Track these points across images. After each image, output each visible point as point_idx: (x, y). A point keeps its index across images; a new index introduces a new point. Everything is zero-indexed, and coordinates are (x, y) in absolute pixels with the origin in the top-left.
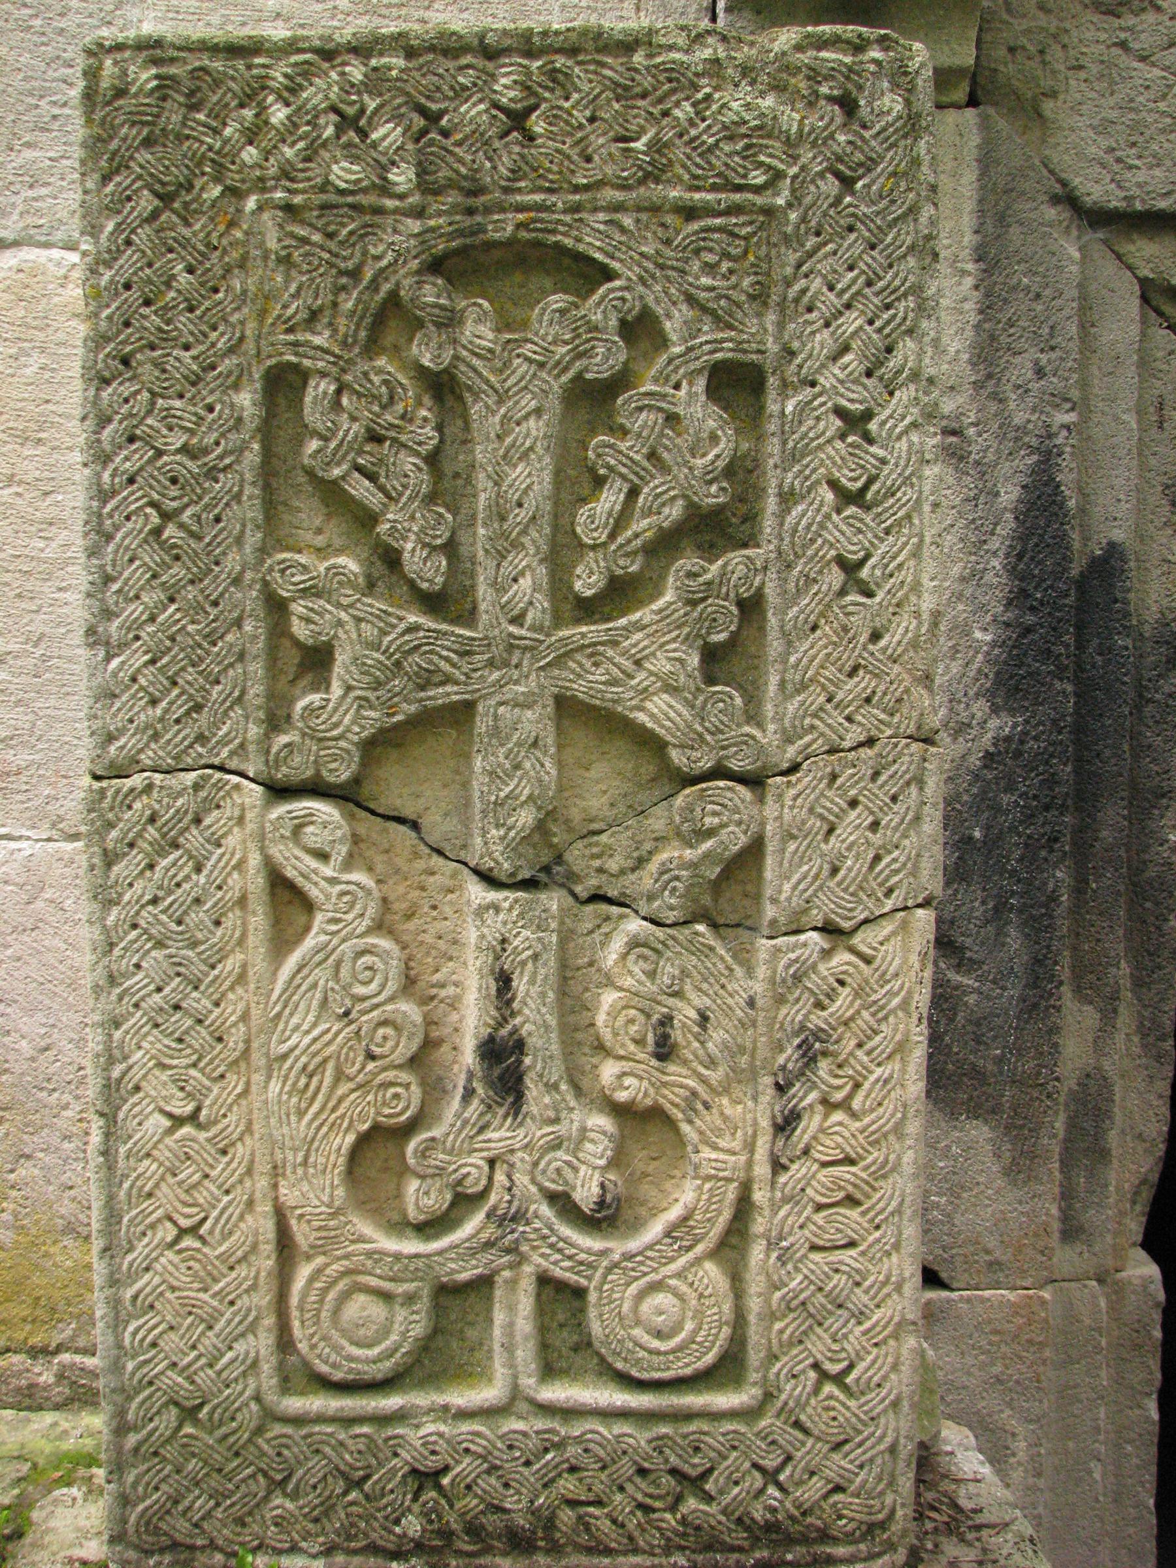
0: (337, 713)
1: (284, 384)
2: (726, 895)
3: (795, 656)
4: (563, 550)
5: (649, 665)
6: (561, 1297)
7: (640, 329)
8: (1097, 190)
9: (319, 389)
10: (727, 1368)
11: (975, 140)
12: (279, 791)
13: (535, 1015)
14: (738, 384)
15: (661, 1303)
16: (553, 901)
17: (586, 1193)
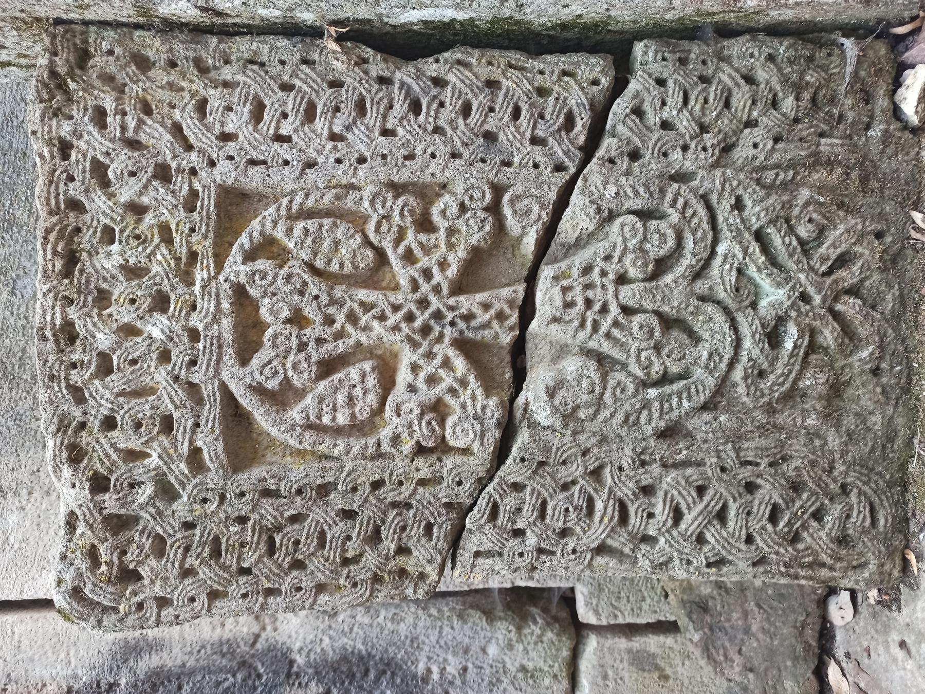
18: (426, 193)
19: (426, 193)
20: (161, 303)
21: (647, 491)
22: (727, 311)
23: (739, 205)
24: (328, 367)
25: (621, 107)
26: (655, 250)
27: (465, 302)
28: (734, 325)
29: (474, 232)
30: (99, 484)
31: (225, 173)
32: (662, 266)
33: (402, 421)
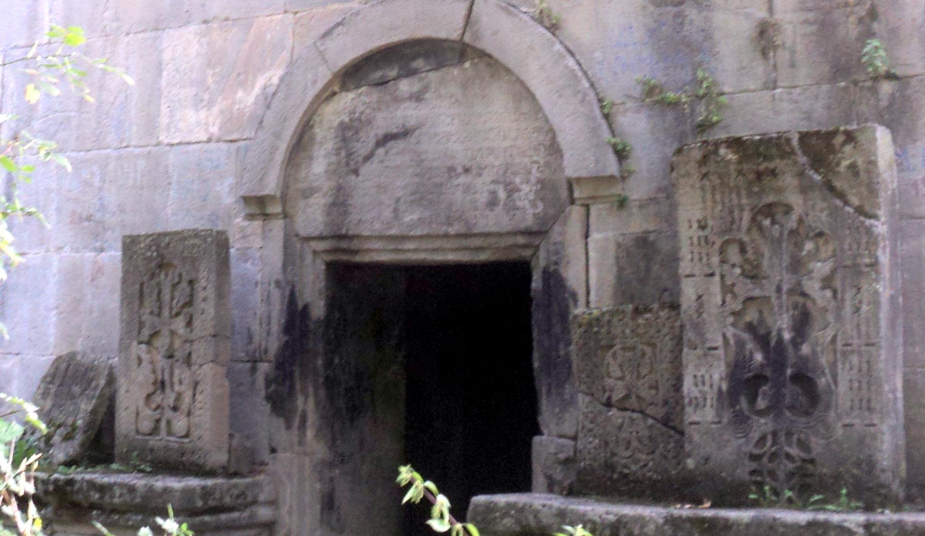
0: (146, 332)
1: (142, 285)
2: (188, 361)
3: (197, 323)
4: (171, 309)
5: (179, 325)
6: (169, 423)
7: (180, 275)
8: (303, 233)
9: (146, 285)
10: (187, 436)
11: (283, 226)
12: (141, 343)
13: (167, 377)
14: (191, 282)
15: (180, 424)
16: (170, 360)
17: (172, 405)
18: (657, 388)
19: (657, 388)
20: (633, 331)
21: (595, 436)
22: (630, 457)
23: (653, 459)
24: (621, 366)
25: (672, 432)
26: (643, 440)
27: (634, 397)
28: (628, 458)
29: (648, 399)
30: (598, 319)
31: (659, 345)
32: (640, 441)
33: (609, 382)
